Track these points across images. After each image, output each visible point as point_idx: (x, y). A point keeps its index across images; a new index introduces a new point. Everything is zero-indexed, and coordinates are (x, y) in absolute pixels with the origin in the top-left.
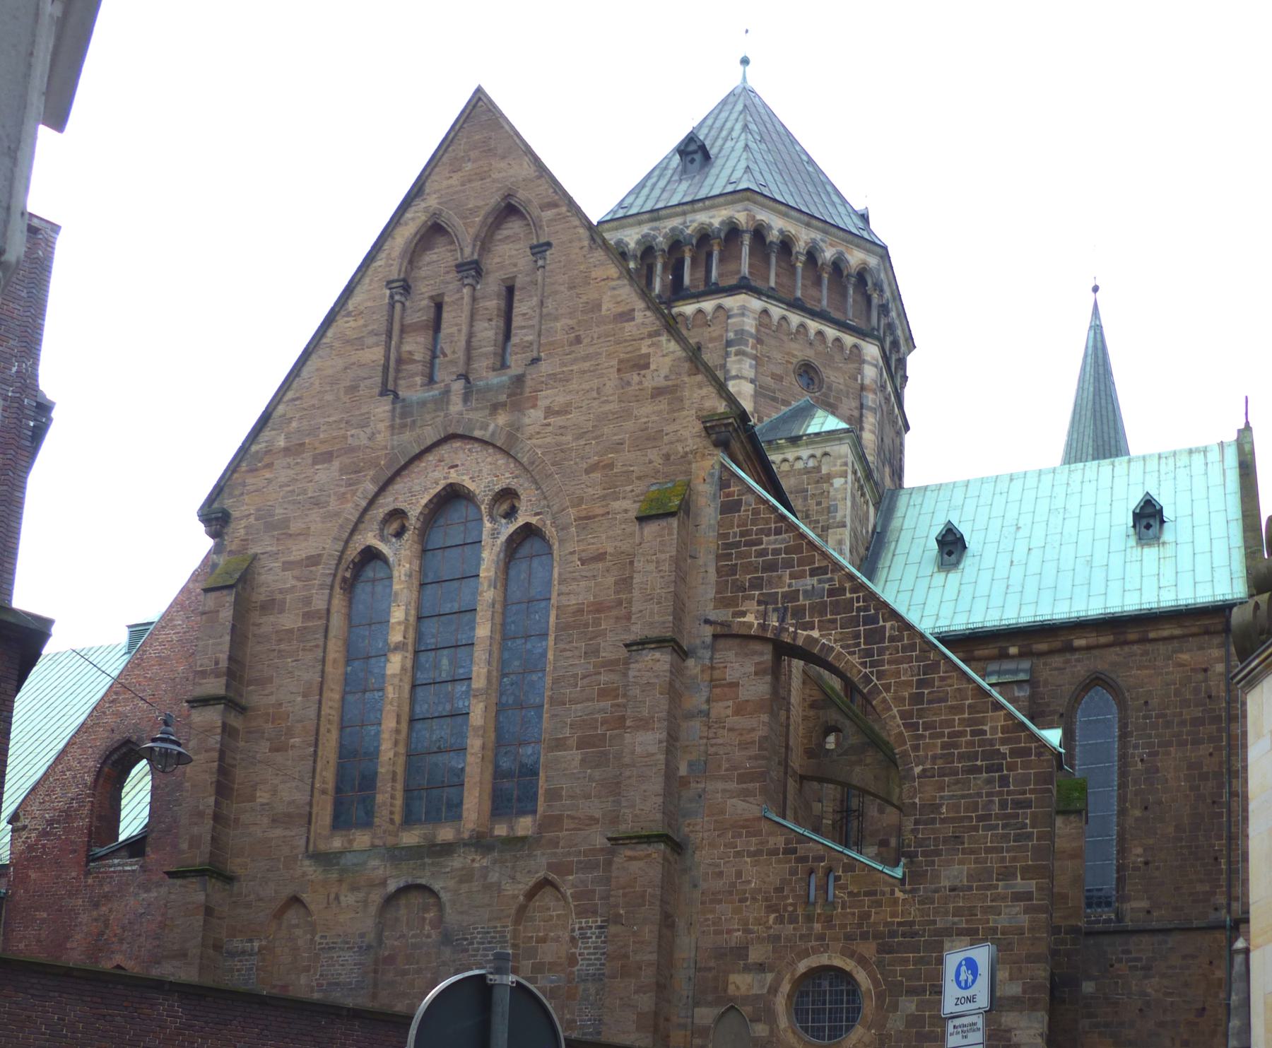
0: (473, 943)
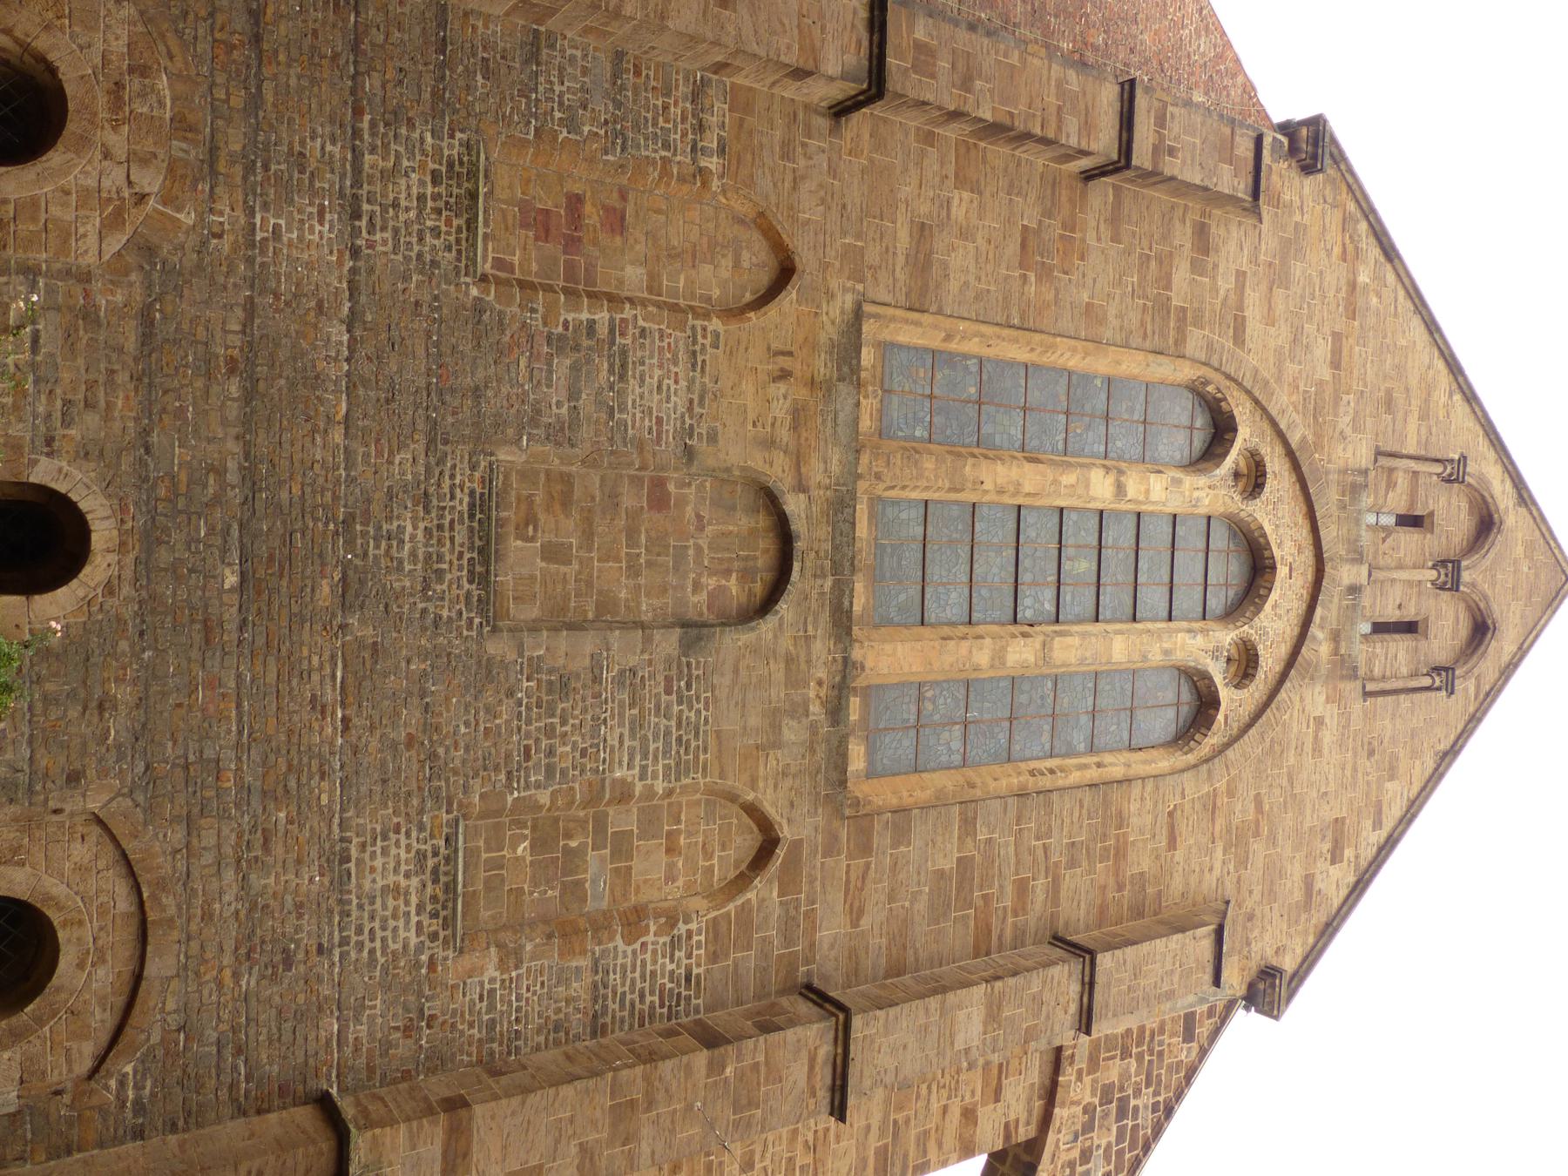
0: (680, 703)
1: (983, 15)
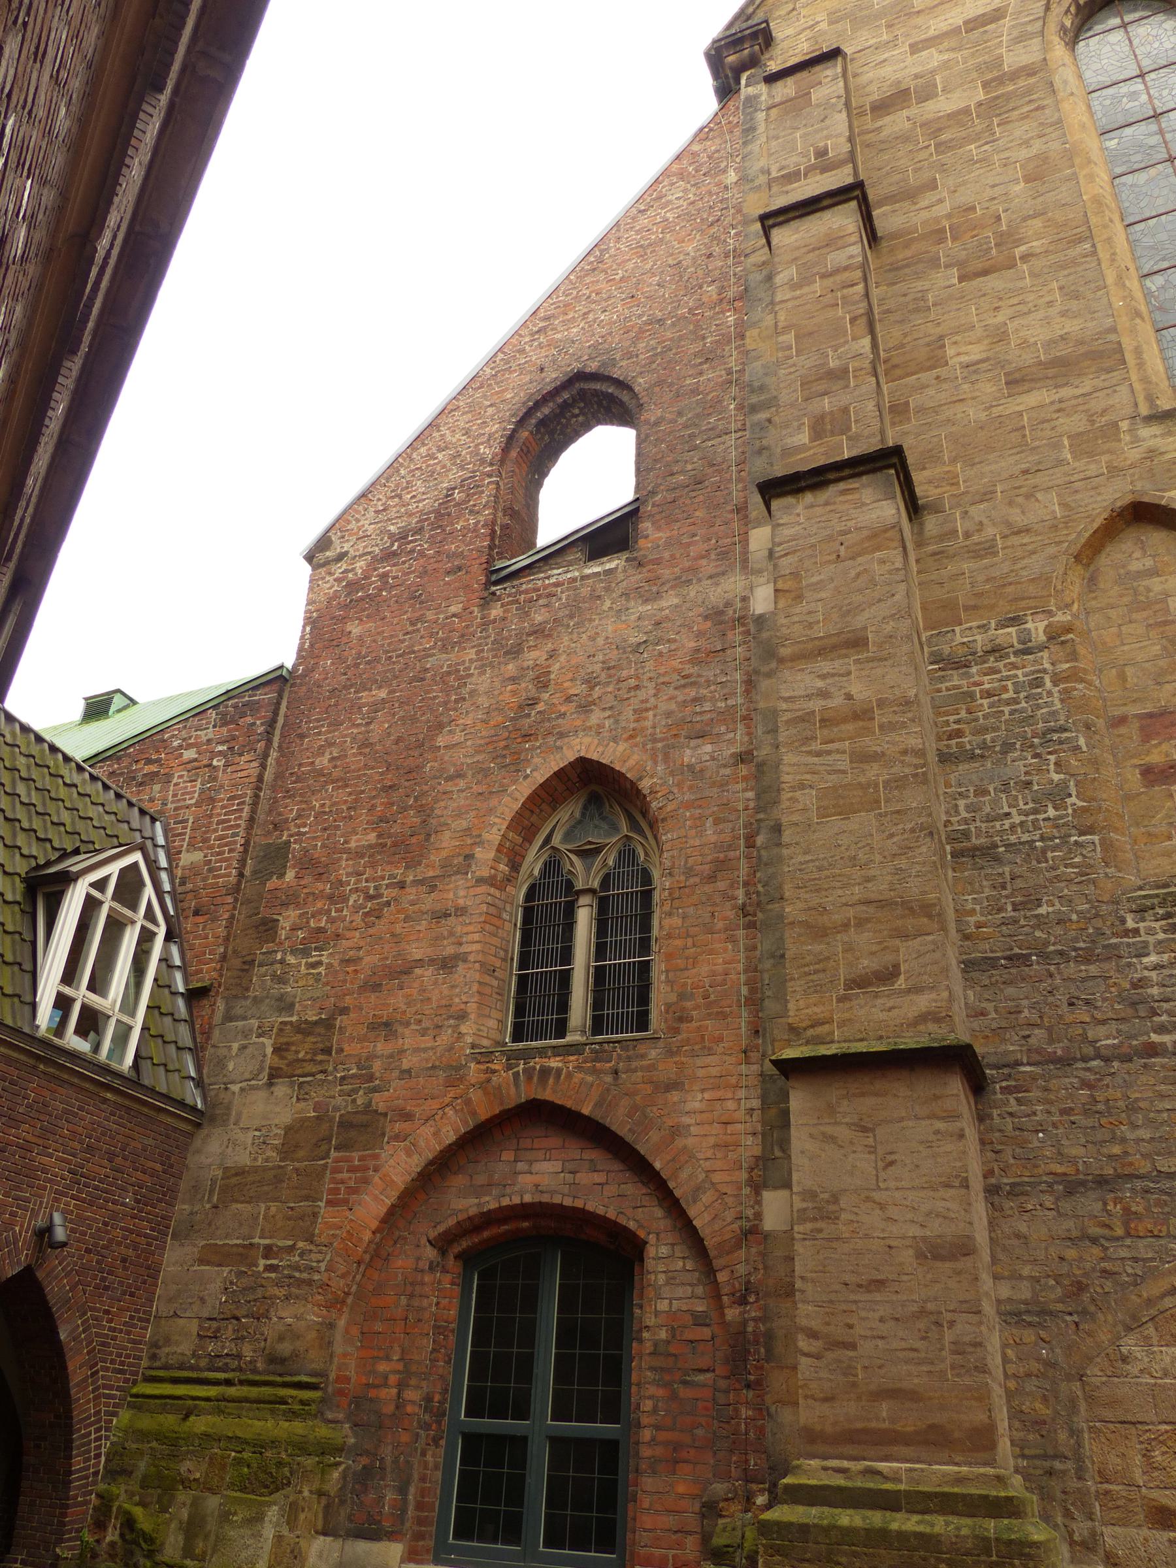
1: (732, 407)
